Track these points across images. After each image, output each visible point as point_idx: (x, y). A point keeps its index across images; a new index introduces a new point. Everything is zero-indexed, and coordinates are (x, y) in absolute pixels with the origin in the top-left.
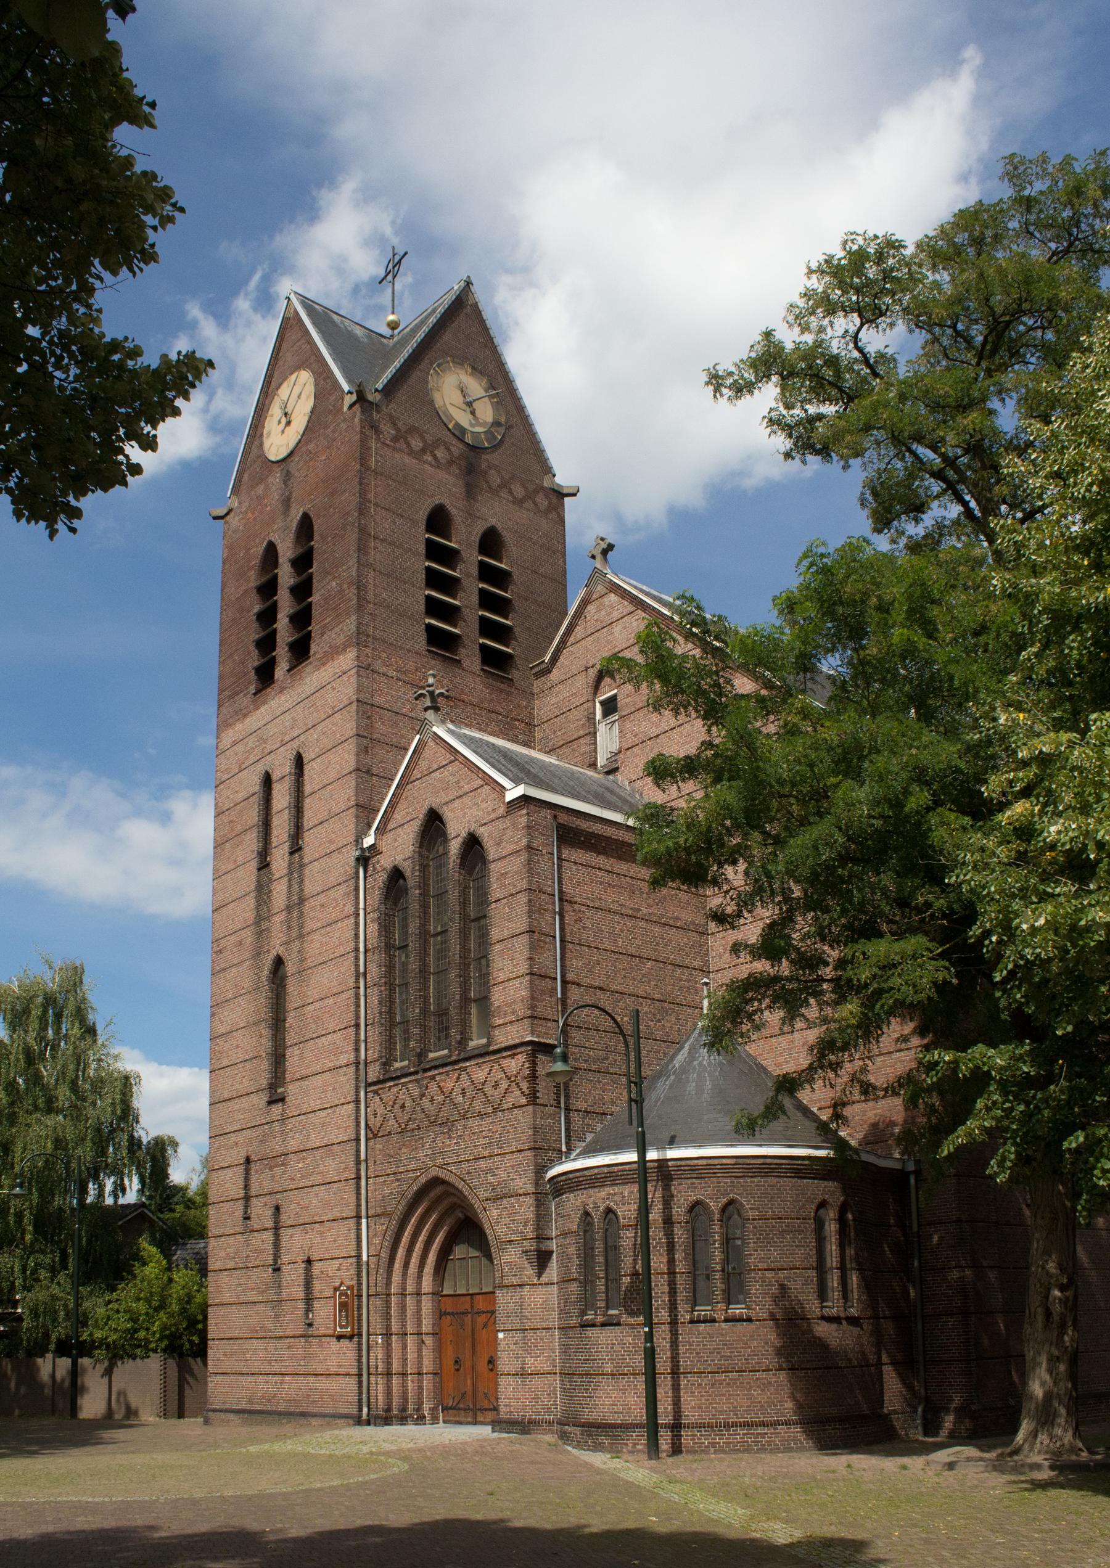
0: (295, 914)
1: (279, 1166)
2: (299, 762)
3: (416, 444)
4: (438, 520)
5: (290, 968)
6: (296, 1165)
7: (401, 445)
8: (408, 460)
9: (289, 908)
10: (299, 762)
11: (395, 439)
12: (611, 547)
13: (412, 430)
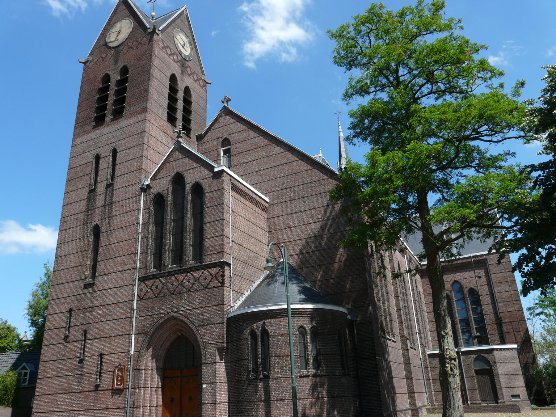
0: (107, 208)
2: (115, 152)
3: (169, 52)
4: (173, 78)
5: (102, 230)
6: (96, 312)
7: (164, 50)
8: (166, 56)
9: (104, 206)
11: (163, 48)
12: (230, 100)
13: (168, 47)
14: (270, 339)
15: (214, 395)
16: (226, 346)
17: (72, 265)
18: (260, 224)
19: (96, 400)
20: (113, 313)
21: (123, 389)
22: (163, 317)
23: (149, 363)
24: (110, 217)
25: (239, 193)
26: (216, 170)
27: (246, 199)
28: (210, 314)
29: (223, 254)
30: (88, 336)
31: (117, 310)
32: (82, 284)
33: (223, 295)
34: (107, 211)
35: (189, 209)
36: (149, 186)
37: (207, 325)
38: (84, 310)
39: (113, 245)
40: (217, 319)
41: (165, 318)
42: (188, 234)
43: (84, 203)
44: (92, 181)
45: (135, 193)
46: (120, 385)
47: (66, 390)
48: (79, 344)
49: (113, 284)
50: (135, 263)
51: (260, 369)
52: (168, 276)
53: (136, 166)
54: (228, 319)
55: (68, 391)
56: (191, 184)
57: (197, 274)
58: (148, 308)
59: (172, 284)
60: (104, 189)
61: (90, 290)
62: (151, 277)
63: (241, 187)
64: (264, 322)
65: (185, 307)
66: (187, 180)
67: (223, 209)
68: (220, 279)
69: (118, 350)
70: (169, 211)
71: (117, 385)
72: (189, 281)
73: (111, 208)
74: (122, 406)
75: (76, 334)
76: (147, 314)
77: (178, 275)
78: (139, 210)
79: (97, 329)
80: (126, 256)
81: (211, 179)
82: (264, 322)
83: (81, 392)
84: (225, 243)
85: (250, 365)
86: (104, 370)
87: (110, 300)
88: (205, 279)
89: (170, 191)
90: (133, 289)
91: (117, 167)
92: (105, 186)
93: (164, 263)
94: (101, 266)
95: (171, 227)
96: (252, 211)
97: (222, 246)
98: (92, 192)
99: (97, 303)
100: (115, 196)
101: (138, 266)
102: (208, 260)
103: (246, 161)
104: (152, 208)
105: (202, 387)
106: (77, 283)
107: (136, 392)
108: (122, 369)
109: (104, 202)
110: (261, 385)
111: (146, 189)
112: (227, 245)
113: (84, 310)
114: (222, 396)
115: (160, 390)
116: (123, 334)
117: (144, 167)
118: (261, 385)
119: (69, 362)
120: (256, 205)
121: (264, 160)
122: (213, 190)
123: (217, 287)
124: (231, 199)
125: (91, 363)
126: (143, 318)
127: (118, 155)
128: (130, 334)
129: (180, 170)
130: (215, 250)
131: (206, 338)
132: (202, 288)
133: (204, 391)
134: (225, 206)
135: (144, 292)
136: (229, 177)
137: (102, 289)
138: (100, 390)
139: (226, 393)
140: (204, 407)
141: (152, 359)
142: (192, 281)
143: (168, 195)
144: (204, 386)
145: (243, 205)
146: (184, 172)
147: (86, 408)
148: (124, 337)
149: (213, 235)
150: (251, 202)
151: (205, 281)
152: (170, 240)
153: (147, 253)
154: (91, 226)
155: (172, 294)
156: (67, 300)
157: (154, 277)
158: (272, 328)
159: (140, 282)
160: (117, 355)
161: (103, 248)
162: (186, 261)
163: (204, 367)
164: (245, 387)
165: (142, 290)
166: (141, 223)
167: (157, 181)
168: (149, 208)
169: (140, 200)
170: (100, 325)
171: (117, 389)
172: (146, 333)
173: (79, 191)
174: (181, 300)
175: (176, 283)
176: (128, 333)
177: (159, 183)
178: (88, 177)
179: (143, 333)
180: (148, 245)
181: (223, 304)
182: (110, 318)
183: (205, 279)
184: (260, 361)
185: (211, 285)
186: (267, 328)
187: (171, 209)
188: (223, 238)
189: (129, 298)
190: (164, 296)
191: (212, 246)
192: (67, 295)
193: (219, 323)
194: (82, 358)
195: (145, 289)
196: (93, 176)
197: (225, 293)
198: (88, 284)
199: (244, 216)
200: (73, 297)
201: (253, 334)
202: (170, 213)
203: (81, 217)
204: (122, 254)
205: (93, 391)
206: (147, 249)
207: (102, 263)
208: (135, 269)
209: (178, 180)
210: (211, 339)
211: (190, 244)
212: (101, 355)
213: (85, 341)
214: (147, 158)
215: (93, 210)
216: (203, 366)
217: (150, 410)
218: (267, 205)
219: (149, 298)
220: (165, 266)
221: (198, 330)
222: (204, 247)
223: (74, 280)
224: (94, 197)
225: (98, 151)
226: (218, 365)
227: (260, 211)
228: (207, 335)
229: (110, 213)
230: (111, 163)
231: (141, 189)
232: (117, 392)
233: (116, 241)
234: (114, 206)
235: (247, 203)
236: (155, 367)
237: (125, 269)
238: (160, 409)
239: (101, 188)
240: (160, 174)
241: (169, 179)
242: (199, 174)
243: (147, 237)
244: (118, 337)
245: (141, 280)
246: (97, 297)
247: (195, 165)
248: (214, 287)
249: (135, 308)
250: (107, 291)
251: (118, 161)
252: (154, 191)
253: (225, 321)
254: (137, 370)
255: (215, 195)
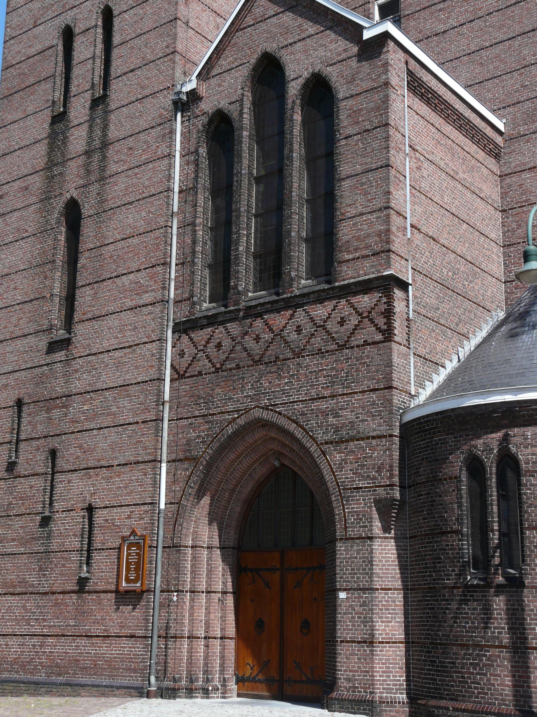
0: (96, 157)
1: (60, 407)
2: (108, 15)
5: (86, 210)
6: (77, 407)
9: (88, 153)
10: (108, 15)
14: (524, 480)
15: (368, 621)
16: (397, 495)
17: (20, 298)
18: (480, 190)
19: (81, 613)
20: (114, 409)
21: (143, 592)
22: (234, 419)
23: (202, 531)
24: (102, 179)
25: (428, 102)
26: (367, 35)
27: (446, 118)
28: (354, 412)
29: (389, 258)
30: (61, 463)
31: (125, 403)
32: (43, 342)
33: (389, 364)
34: (95, 165)
35: (296, 146)
36: (194, 96)
37: (347, 441)
38: (50, 402)
39: (111, 247)
40: (373, 426)
41: (241, 421)
42: (295, 208)
43: (42, 149)
44: (57, 94)
45: (161, 116)
46: (135, 581)
47: (14, 586)
48: (39, 483)
49: (113, 341)
50: (165, 288)
51: (497, 560)
52: (245, 317)
53: (159, 45)
54: (404, 427)
55: (19, 590)
56: (301, 81)
57: (320, 311)
58: (199, 397)
59: (257, 339)
60: (87, 112)
61: (60, 355)
62: (205, 322)
63: (433, 84)
64: (506, 435)
65: (292, 394)
66: (291, 71)
67: (387, 138)
68: (381, 321)
69: (128, 500)
70: (245, 154)
71: (128, 581)
72: (299, 330)
73: (104, 157)
74: (140, 633)
75: (32, 458)
76: (197, 413)
77: (272, 316)
78: (170, 156)
79: (80, 447)
80: (143, 273)
81: (353, 63)
82: (506, 435)
83: (46, 593)
84: (394, 229)
85: (467, 548)
86: (97, 545)
87: (109, 379)
88: (342, 322)
89: (247, 104)
90: (162, 350)
91: (115, 53)
92: (88, 105)
93: (236, 286)
94: (84, 298)
95: (250, 195)
96: (462, 154)
97: (386, 236)
98: (59, 118)
99: (77, 386)
100: (112, 127)
101: (172, 295)
102: (348, 274)
103: (441, 28)
104: (203, 151)
105: (336, 597)
106: (31, 340)
107: (171, 600)
108: (138, 543)
109: (89, 144)
110: (499, 603)
111: (186, 104)
112: (400, 234)
113: (50, 402)
114: (390, 623)
115: (230, 600)
116: (140, 459)
117: (180, 47)
118: (499, 603)
119: (18, 523)
120: (472, 139)
121: (494, 19)
122: (358, 90)
123: (374, 343)
124: (406, 113)
125: (68, 528)
126: (185, 422)
127: (116, 22)
128: (156, 461)
129: (271, 47)
130: (367, 247)
131: (346, 475)
132: (334, 347)
133: (342, 609)
134: (392, 132)
135: (187, 358)
136: (401, 55)
137: (88, 352)
138: (89, 592)
139: (400, 618)
140: (342, 650)
141: (210, 523)
142: (308, 329)
143: (241, 113)
144: (342, 595)
145: (438, 135)
146: (283, 51)
147: (58, 631)
148: (142, 466)
149: (360, 209)
150: (459, 128)
151: (342, 329)
152: (248, 228)
153: (193, 263)
154: (59, 204)
155: (256, 363)
156: (11, 380)
157: (212, 321)
158: (529, 450)
159: (177, 335)
160: (127, 510)
161: (87, 254)
162: (292, 279)
163: (340, 547)
164: (454, 606)
165: (182, 354)
166: (176, 189)
167: (214, 82)
168: (196, 151)
169: (172, 132)
170: (85, 439)
171: (127, 592)
172: (195, 460)
173: (30, 121)
174: (280, 377)
175: (267, 336)
176: (151, 458)
177: (220, 85)
178: (47, 86)
179: (187, 459)
180: (194, 242)
181: (390, 388)
182: (107, 421)
183: (342, 322)
184: (495, 538)
185: (359, 338)
186: (514, 450)
187: (251, 150)
188: (388, 216)
189: (153, 373)
190: (238, 367)
191: (358, 239)
192: (10, 369)
193: (379, 437)
194: (47, 514)
195: (189, 351)
196: (60, 82)
197: (396, 359)
198: (56, 342)
199: (442, 165)
200: (23, 373)
201: (475, 467)
202: (248, 159)
203: (37, 182)
204: (134, 266)
205: (73, 592)
206: (194, 252)
207: (88, 291)
208: (164, 301)
209: (268, 72)
210: (359, 477)
211: (300, 237)
212: (90, 509)
213: (53, 474)
214: (187, 23)
215: (63, 163)
216: (338, 544)
217: (207, 646)
218: (499, 140)
219: (200, 373)
220: (239, 293)
221: (324, 453)
222: (337, 239)
223: (26, 331)
224: (63, 133)
225: (67, 18)
226: (377, 545)
227: (481, 155)
228: (349, 467)
229: (103, 169)
230: (100, 46)
231: (175, 103)
232: (128, 598)
233: (119, 237)
234: (111, 152)
235: (448, 129)
236: (216, 542)
237: (141, 302)
238: (231, 645)
239: (79, 110)
240: (222, 62)
241: (245, 72)
242: (321, 52)
243: (193, 224)
244: (127, 468)
245: (182, 328)
246: (76, 371)
247: (311, 28)
248: (366, 343)
249: (167, 397)
250: (101, 356)
251: (116, 39)
252: (207, 106)
253: (397, 432)
254: (174, 547)
255: (364, 103)
